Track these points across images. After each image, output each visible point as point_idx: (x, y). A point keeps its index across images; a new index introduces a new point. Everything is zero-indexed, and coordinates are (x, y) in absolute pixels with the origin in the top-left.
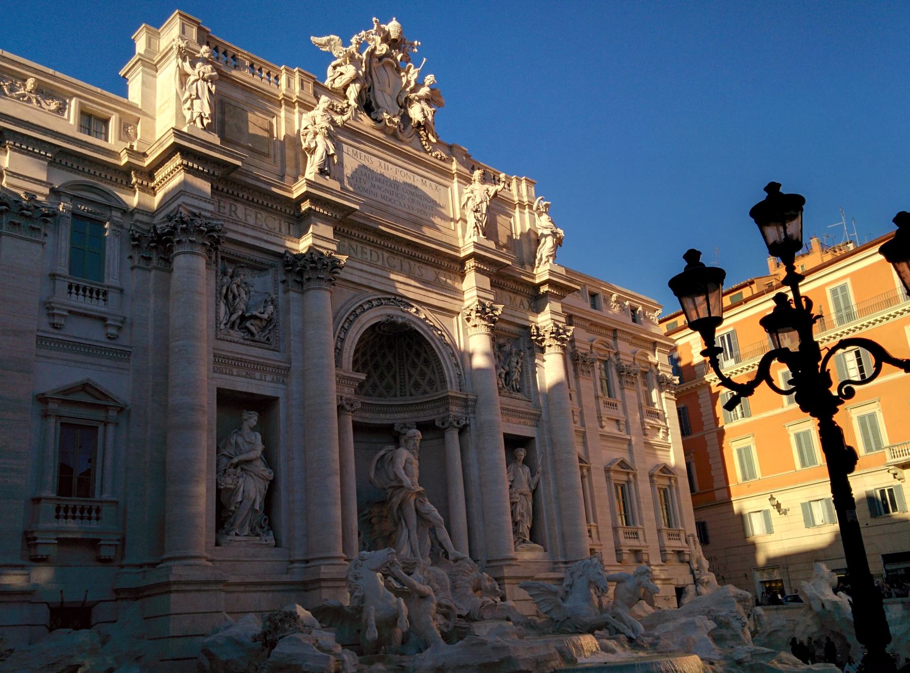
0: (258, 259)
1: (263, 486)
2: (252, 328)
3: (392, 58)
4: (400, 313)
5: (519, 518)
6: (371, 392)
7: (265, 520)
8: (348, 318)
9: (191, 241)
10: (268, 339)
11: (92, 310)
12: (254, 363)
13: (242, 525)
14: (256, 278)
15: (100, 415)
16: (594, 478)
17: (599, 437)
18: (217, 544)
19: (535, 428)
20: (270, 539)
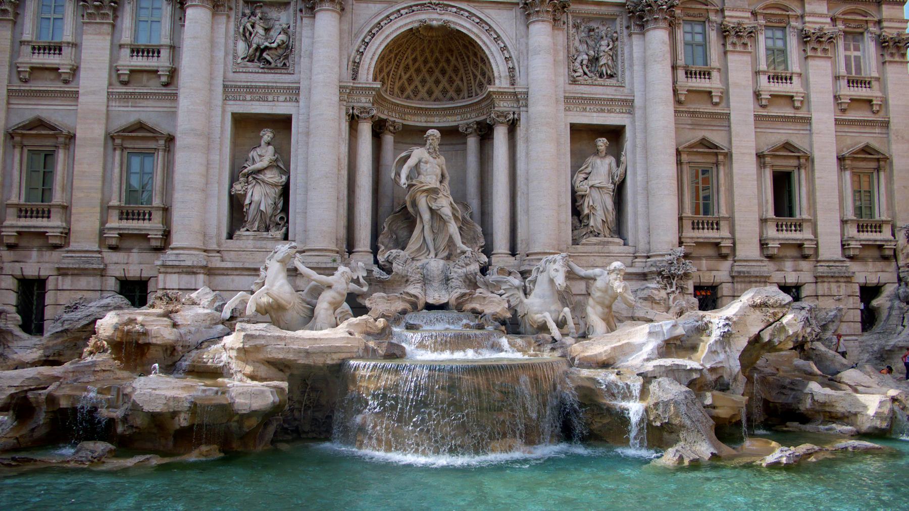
1: (274, 192)
2: (269, 58)
4: (435, 16)
5: (586, 211)
6: (440, 96)
7: (282, 218)
8: (370, 31)
10: (285, 64)
12: (264, 87)
13: (254, 220)
15: (152, 145)
16: (735, 165)
17: (752, 118)
18: (230, 236)
19: (626, 115)
20: (279, 234)
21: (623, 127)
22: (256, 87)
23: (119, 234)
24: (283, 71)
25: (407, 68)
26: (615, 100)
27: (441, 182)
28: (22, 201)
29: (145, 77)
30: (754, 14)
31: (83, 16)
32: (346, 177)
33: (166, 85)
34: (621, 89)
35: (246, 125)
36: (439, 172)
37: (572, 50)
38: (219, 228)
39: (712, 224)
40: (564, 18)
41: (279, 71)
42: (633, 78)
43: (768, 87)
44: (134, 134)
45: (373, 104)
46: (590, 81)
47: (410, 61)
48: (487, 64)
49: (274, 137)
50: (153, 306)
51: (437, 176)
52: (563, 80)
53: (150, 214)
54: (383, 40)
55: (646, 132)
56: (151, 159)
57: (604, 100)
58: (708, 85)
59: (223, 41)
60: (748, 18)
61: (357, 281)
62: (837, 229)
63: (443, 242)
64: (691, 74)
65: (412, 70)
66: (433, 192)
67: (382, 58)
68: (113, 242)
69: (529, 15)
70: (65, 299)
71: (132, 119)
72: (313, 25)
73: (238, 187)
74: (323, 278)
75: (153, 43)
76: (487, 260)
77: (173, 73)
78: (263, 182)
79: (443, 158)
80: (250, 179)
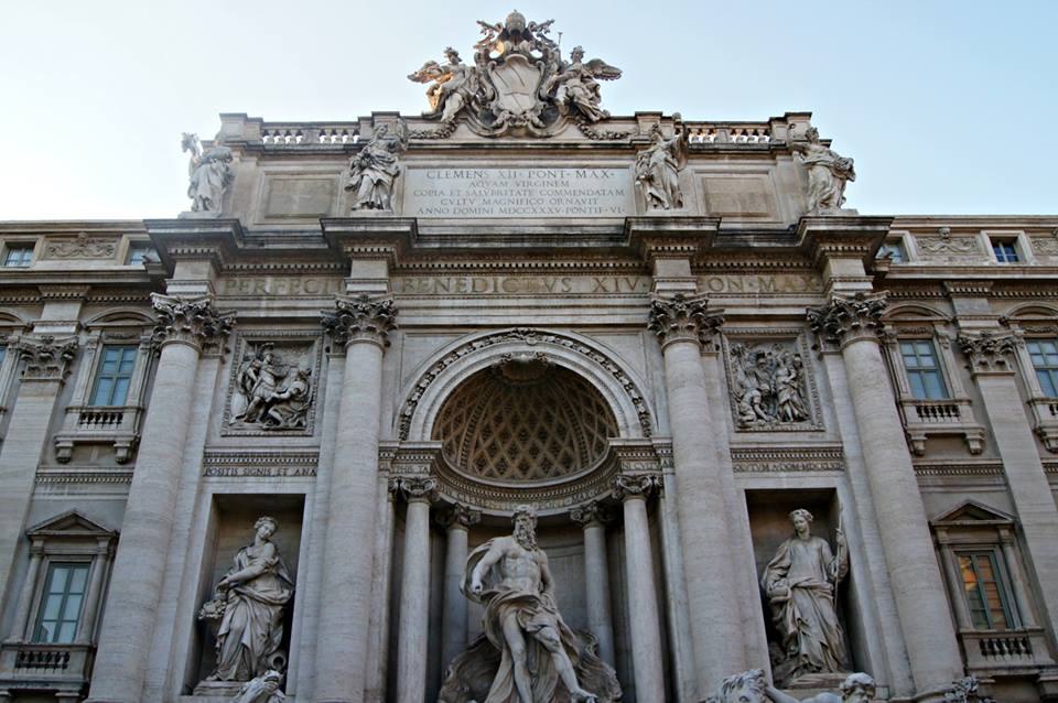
0: (294, 333)
1: (268, 615)
2: (276, 415)
3: (517, 52)
4: (525, 348)
5: (791, 629)
6: (542, 473)
7: (278, 661)
8: (428, 373)
9: (171, 331)
10: (300, 424)
11: (98, 436)
12: (265, 455)
14: (304, 356)
15: (88, 548)
16: (1031, 544)
17: (1041, 470)
18: (189, 690)
21: (834, 490)
22: (253, 455)
23: (10, 690)
24: (296, 433)
25: (487, 432)
26: (812, 450)
27: (541, 592)
29: (95, 451)
30: (1004, 323)
31: (23, 373)
32: (385, 587)
34: (820, 434)
35: (233, 512)
36: (536, 572)
37: (736, 387)
38: (170, 674)
39: (1016, 643)
40: (716, 340)
41: (290, 433)
42: (834, 416)
44: (62, 533)
45: (430, 474)
46: (768, 427)
48: (607, 413)
49: (277, 528)
51: (533, 578)
52: (725, 423)
53: (67, 659)
54: (448, 384)
55: (871, 495)
56: (85, 571)
57: (795, 450)
58: (960, 425)
59: (211, 392)
60: (997, 328)
64: (927, 412)
65: (495, 435)
66: (524, 602)
67: (446, 412)
69: (662, 336)
71: (66, 509)
72: (343, 367)
73: (211, 608)
75: (115, 405)
77: (134, 446)
78: (252, 598)
79: (542, 552)
80: (232, 594)
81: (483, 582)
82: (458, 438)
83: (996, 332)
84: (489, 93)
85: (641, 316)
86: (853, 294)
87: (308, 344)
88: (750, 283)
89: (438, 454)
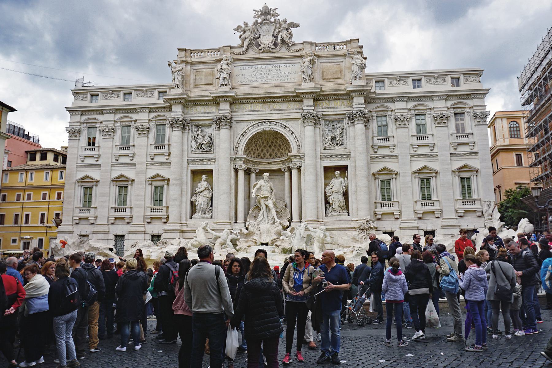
5: (330, 203)
20: (208, 215)
25: (260, 146)
27: (270, 193)
28: (116, 206)
33: (168, 159)
36: (269, 189)
43: (415, 141)
47: (261, 143)
50: (157, 246)
61: (236, 234)
62: (453, 204)
63: (270, 218)
65: (262, 146)
67: (248, 144)
68: (149, 221)
70: (131, 243)
73: (193, 199)
74: (218, 234)
76: (288, 224)
79: (271, 183)
81: (255, 193)
82: (252, 150)
83: (405, 114)
84: (258, 36)
85: (299, 116)
86: (358, 109)
87: (211, 126)
88: (332, 104)
89: (245, 158)
